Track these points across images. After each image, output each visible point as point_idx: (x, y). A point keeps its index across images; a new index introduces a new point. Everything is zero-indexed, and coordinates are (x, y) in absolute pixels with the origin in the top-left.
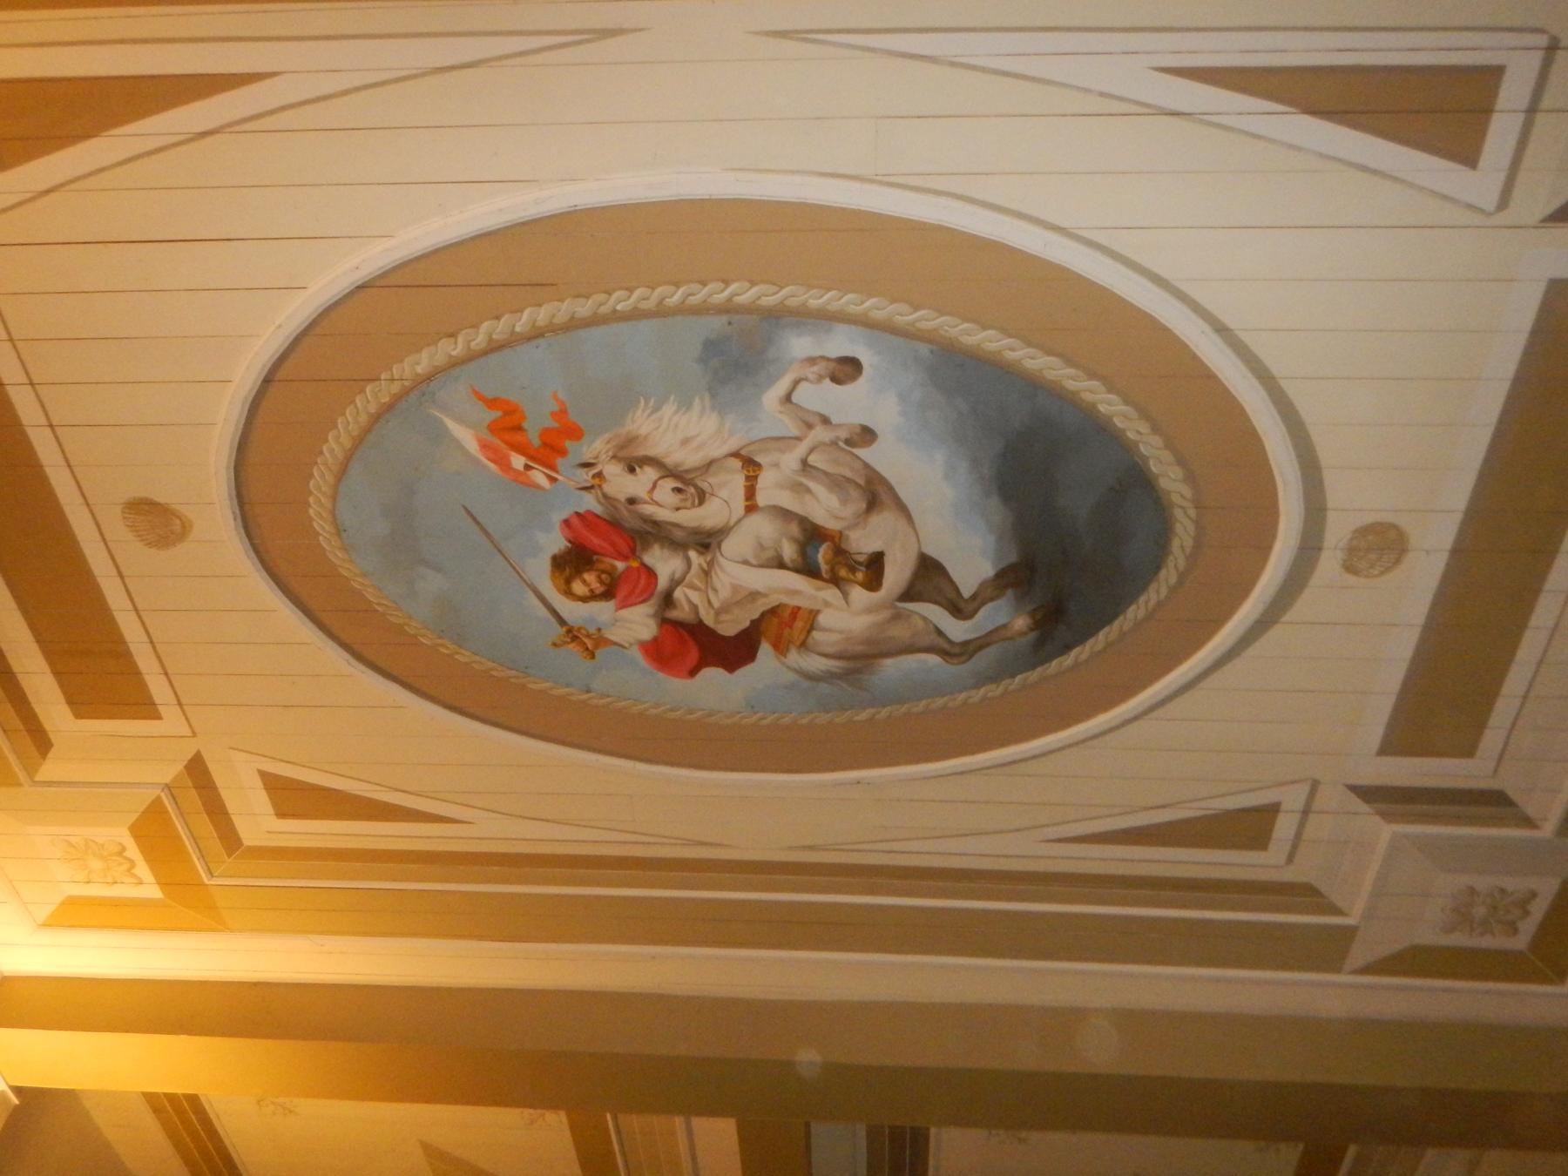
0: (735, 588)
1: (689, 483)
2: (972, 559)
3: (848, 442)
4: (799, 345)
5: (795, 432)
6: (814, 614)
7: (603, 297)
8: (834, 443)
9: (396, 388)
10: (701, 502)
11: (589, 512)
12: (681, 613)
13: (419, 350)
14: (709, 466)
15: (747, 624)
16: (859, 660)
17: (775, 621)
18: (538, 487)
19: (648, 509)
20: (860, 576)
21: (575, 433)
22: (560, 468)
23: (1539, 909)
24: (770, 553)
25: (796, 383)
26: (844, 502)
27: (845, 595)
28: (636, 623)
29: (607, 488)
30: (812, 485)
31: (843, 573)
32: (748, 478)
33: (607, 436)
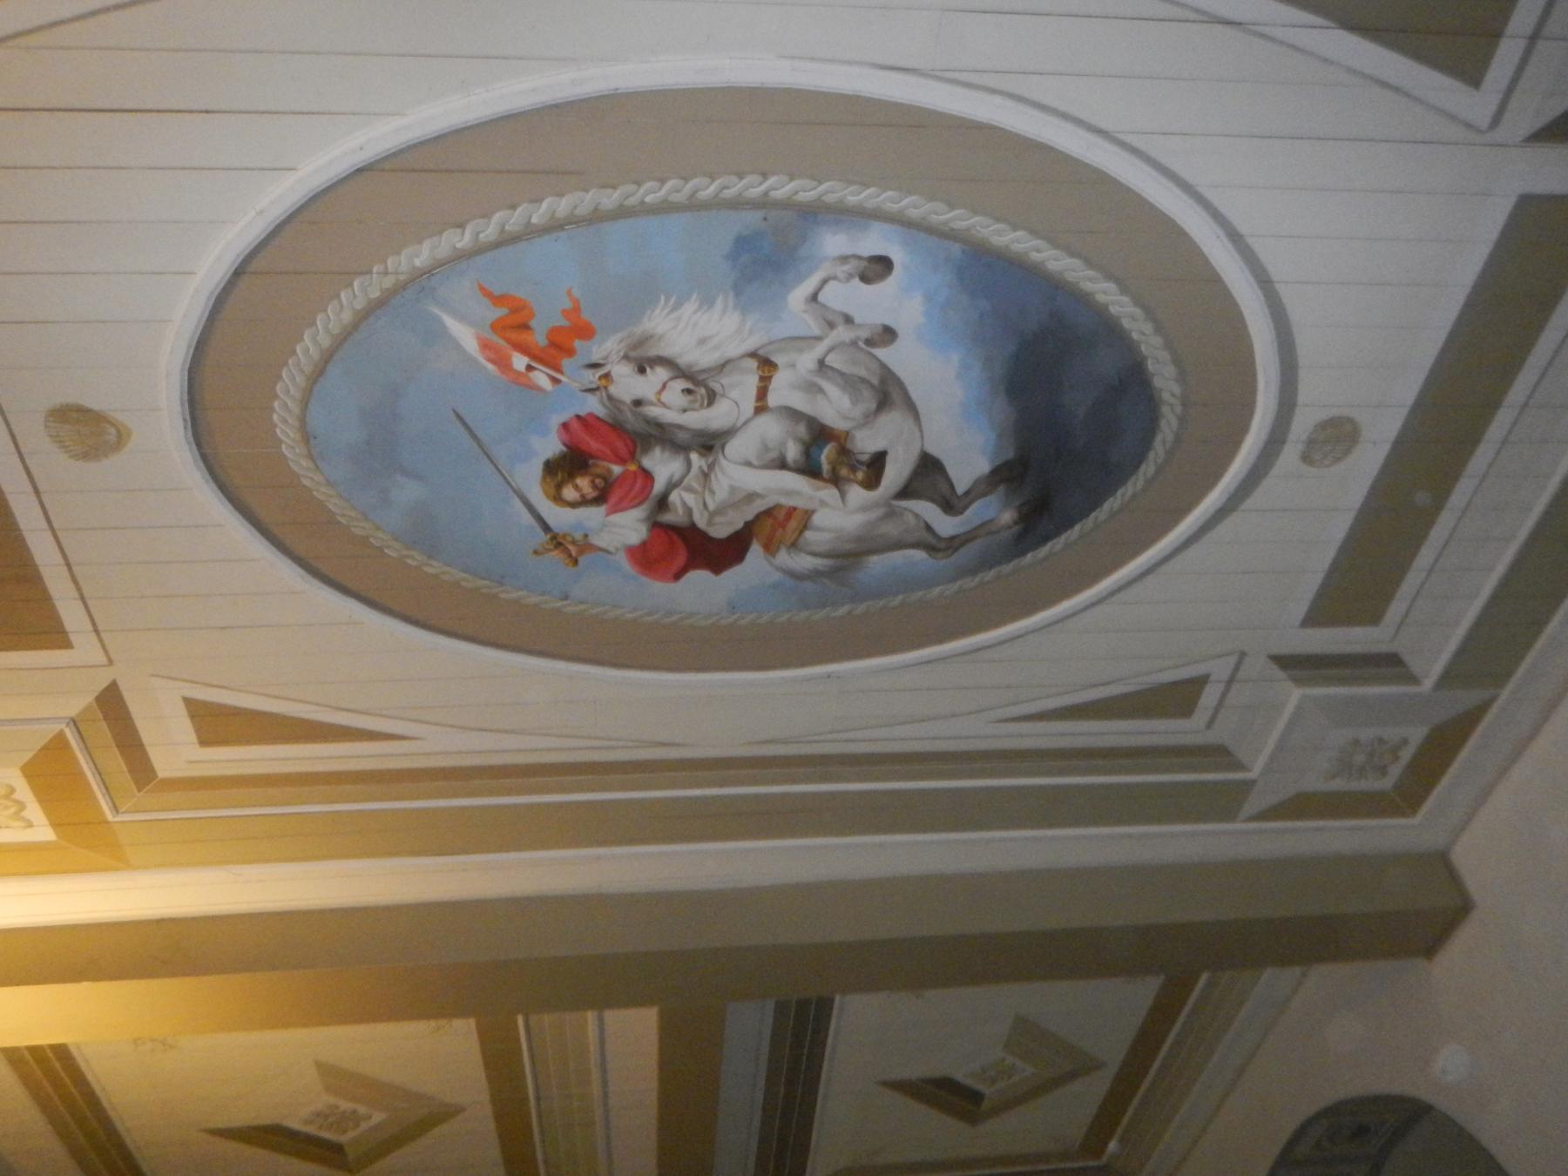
0: (733, 489)
1: (700, 384)
2: (969, 453)
3: (869, 342)
4: (834, 242)
5: (816, 332)
6: (808, 514)
7: (631, 188)
8: (854, 343)
9: (388, 282)
10: (710, 403)
11: (591, 414)
12: (674, 517)
13: (420, 242)
14: (723, 367)
15: (740, 525)
16: (847, 557)
17: (769, 522)
18: (540, 389)
19: (653, 411)
20: (860, 475)
21: (585, 332)
22: (564, 369)
23: (1407, 755)
24: (773, 455)
25: (825, 282)
26: (854, 402)
27: (843, 495)
29: (612, 389)
30: (827, 386)
31: (844, 472)
32: (762, 379)
33: (619, 335)
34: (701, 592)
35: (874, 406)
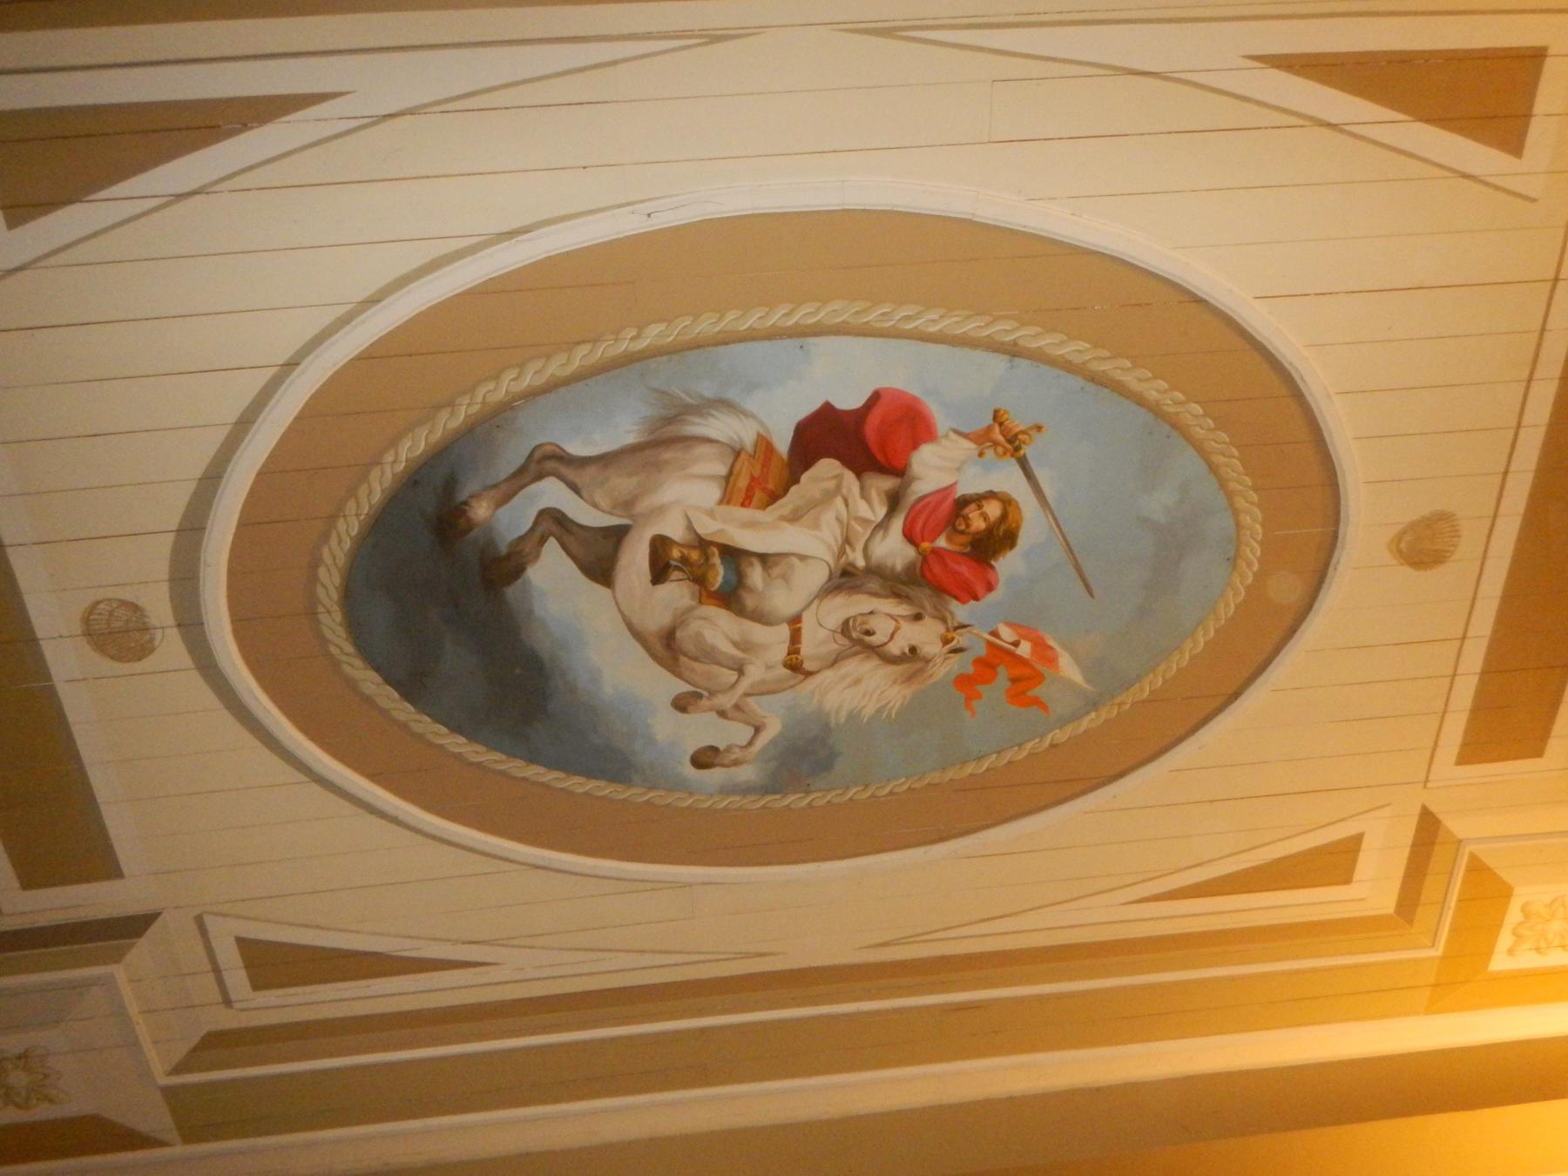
0: (816, 525)
1: (857, 641)
2: (552, 579)
3: (700, 696)
4: (747, 774)
5: (751, 701)
6: (726, 500)
8: (712, 694)
10: (846, 622)
11: (964, 602)
12: (882, 484)
14: (836, 661)
15: (805, 478)
16: (663, 441)
17: (770, 486)
18: (1009, 624)
19: (903, 610)
20: (676, 553)
21: (963, 682)
22: (983, 644)
24: (776, 571)
25: (750, 743)
26: (699, 635)
27: (690, 527)
28: (936, 468)
29: (941, 629)
31: (694, 555)
32: (797, 652)
33: (933, 680)
34: (843, 376)
35: (678, 634)
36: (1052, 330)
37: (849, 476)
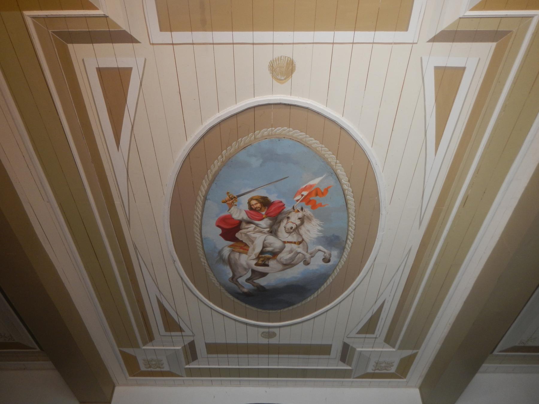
5: (309, 251)
6: (246, 253)
7: (354, 215)
8: (305, 258)
9: (333, 163)
11: (285, 208)
12: (244, 225)
13: (345, 172)
18: (295, 196)
19: (285, 221)
28: (239, 213)
30: (292, 254)
31: (261, 259)
33: (312, 215)
34: (212, 233)
35: (285, 263)
36: (200, 189)
37: (241, 231)
